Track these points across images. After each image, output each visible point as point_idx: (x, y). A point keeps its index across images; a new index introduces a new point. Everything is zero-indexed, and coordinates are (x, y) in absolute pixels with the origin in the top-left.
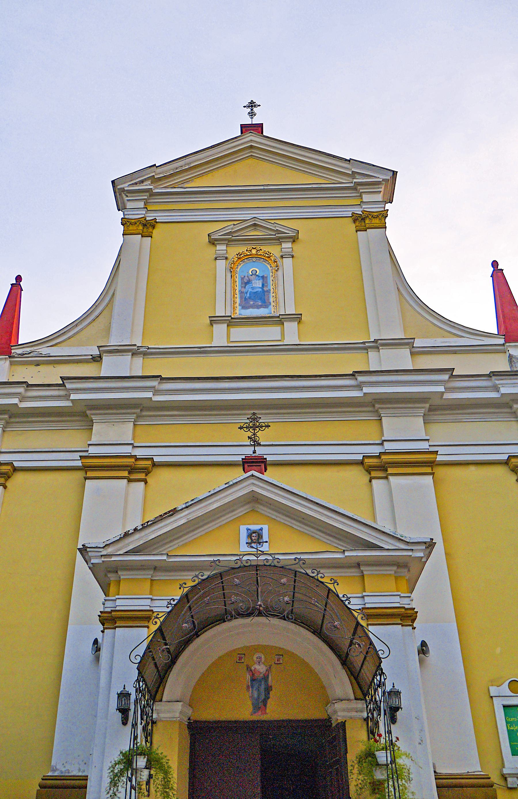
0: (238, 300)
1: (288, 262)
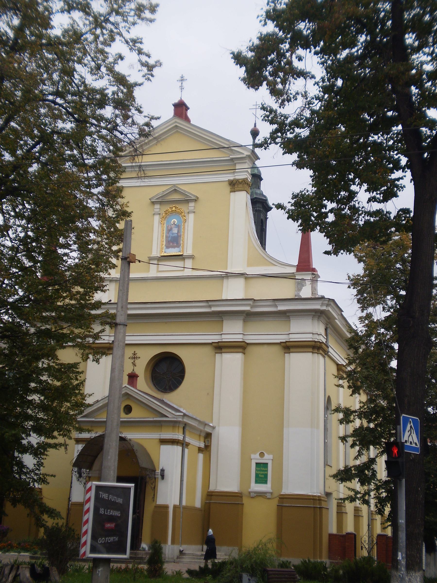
0: (164, 243)
1: (191, 216)
